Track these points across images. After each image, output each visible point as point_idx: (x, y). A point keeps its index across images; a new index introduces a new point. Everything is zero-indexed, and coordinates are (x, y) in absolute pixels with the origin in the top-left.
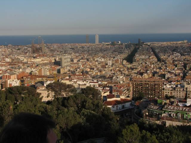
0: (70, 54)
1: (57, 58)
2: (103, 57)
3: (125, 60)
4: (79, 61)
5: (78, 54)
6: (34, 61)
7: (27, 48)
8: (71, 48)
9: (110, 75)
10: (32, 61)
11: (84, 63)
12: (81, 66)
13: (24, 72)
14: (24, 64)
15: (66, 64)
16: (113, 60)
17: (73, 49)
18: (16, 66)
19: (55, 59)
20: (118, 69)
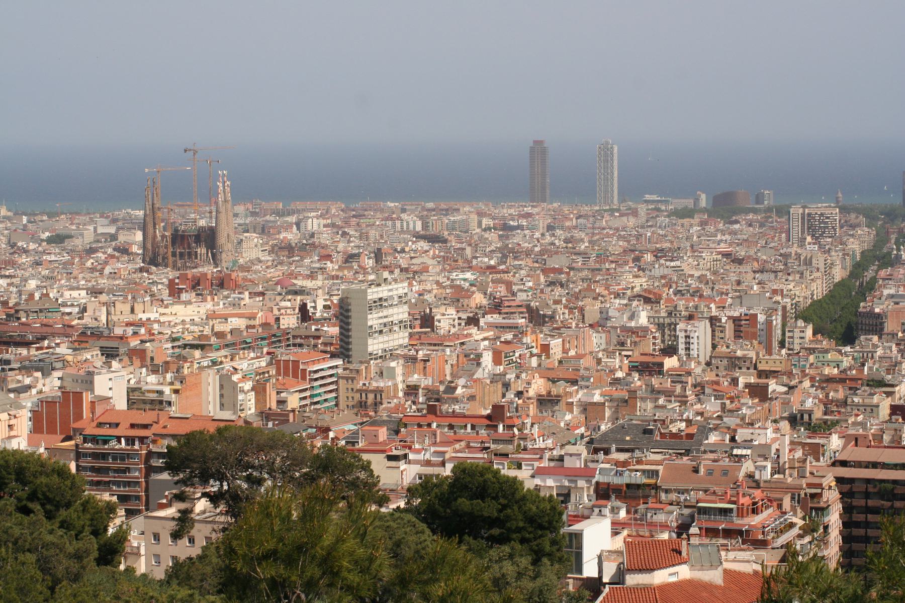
0: (411, 274)
1: (320, 304)
2: (647, 300)
3: (801, 323)
4: (473, 321)
5: (468, 275)
6: (153, 316)
7: (112, 230)
8: (419, 237)
9: (689, 422)
10: (144, 317)
11: (509, 336)
12: (487, 359)
13: (78, 396)
14: (85, 337)
15: (375, 345)
16: (713, 320)
17: (433, 239)
18: (24, 352)
19: (303, 308)
20: (747, 386)
